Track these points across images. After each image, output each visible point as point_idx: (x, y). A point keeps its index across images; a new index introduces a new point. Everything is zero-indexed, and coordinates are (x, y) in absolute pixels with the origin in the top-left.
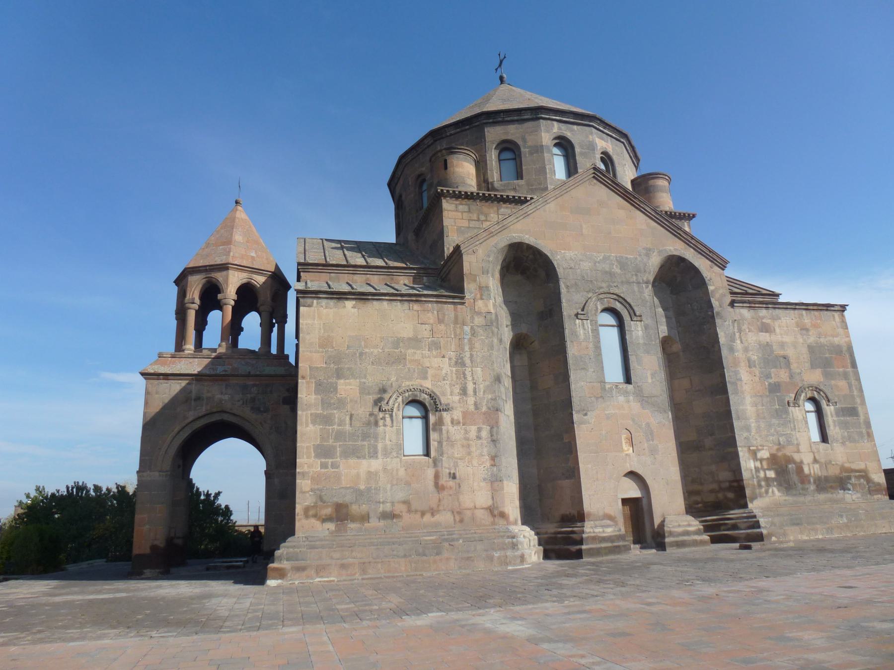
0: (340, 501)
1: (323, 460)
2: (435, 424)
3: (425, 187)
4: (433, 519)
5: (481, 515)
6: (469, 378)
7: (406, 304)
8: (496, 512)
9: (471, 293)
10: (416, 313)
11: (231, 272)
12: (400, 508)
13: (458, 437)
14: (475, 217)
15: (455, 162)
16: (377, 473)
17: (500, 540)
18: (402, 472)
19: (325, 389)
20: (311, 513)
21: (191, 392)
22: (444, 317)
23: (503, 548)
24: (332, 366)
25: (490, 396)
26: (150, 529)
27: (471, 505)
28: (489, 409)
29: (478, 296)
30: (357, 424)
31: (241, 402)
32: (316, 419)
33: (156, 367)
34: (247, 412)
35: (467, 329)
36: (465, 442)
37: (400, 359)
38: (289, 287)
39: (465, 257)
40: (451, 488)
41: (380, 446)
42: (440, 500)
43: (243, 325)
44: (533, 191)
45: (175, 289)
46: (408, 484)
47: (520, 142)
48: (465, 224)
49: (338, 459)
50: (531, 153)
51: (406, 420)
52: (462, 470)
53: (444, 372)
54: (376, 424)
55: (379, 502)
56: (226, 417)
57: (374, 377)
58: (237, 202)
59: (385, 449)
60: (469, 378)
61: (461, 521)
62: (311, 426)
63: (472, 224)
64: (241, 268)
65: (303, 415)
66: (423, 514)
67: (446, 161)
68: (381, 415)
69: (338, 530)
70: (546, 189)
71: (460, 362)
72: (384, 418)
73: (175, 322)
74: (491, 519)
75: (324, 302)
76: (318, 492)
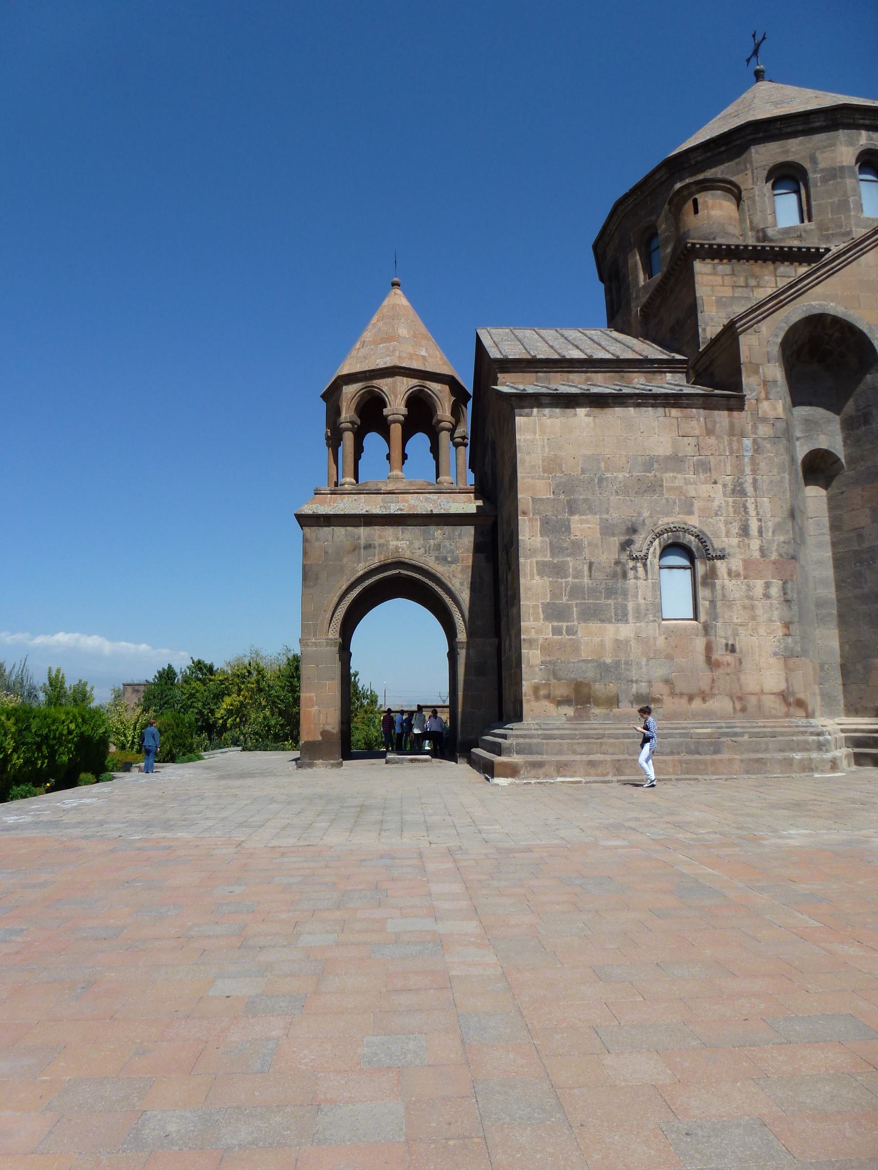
0: (579, 680)
1: (556, 624)
2: (705, 577)
4: (704, 706)
5: (771, 703)
6: (752, 513)
7: (660, 410)
8: (791, 700)
9: (752, 390)
10: (675, 421)
12: (660, 689)
13: (737, 595)
14: (741, 281)
15: (710, 202)
16: (627, 641)
17: (801, 738)
18: (661, 642)
19: (554, 528)
20: (542, 692)
21: (359, 538)
22: (714, 426)
23: (805, 747)
24: (562, 497)
25: (782, 539)
26: (320, 711)
27: (757, 689)
28: (780, 555)
29: (763, 395)
31: (422, 551)
32: (543, 569)
33: (314, 506)
35: (747, 442)
36: (747, 602)
37: (654, 487)
39: (742, 338)
40: (728, 664)
41: (630, 606)
42: (713, 681)
44: (827, 238)
45: (323, 405)
46: (670, 657)
47: (807, 165)
48: (727, 292)
49: (576, 623)
50: (824, 180)
51: (664, 572)
52: (745, 640)
53: (716, 504)
54: (625, 575)
55: (632, 681)
57: (620, 511)
59: (637, 610)
60: (752, 513)
61: (744, 710)
62: (537, 578)
63: (738, 292)
65: (527, 565)
66: (691, 698)
67: (695, 202)
68: (631, 564)
69: (578, 717)
70: (849, 233)
71: (738, 490)
72: (634, 568)
74: (784, 709)
76: (551, 667)
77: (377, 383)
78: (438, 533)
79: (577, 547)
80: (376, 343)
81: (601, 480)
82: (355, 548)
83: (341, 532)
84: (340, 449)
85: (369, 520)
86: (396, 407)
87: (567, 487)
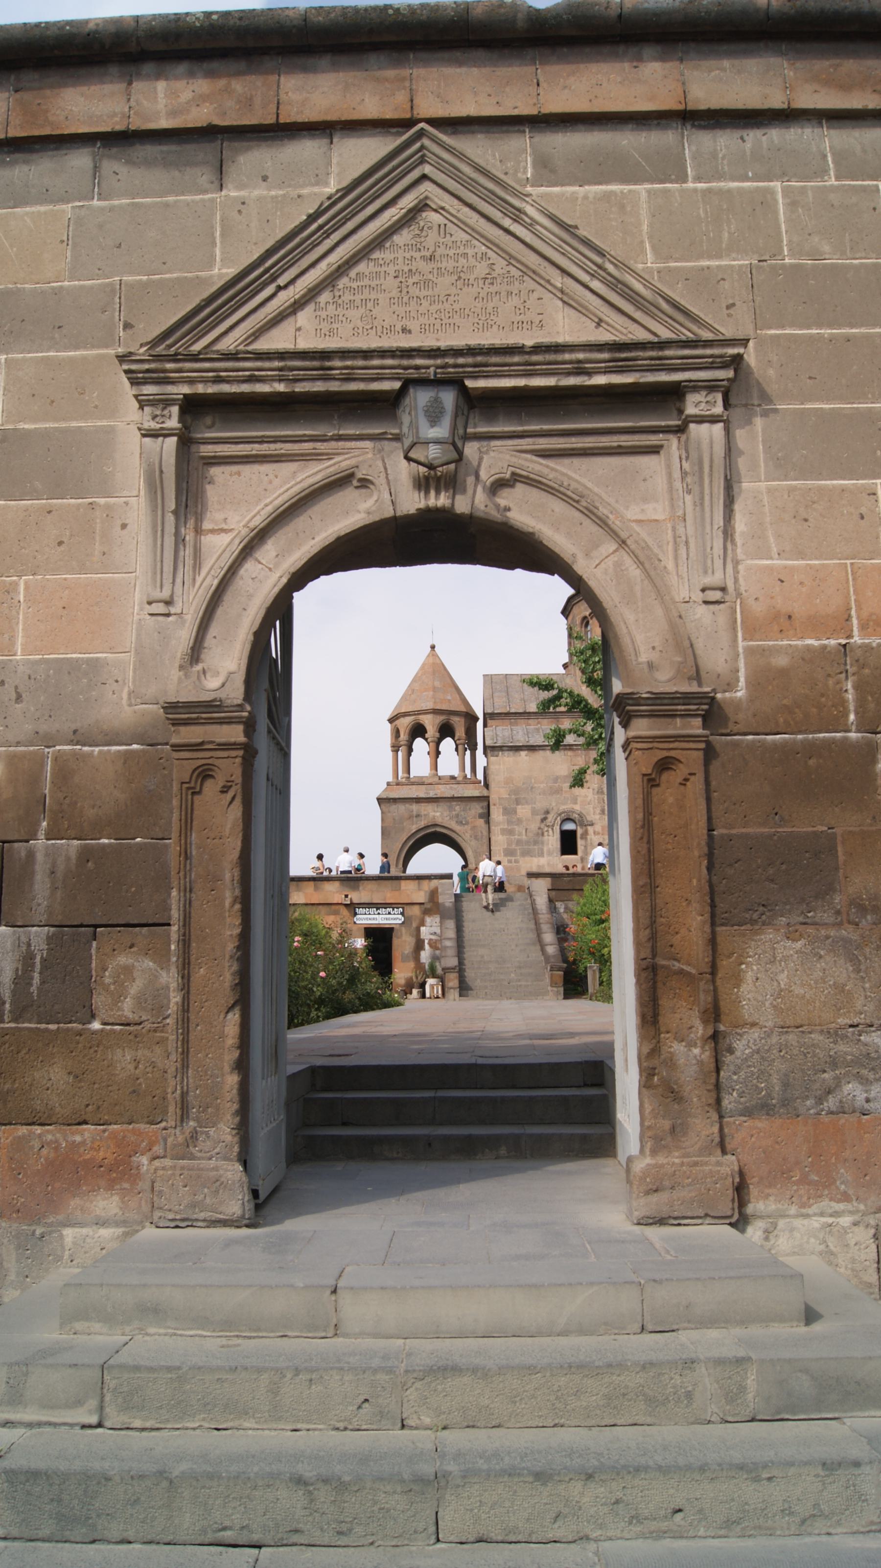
3: (589, 628)
19: (508, 812)
32: (504, 832)
34: (453, 825)
38: (477, 719)
41: (545, 849)
43: (440, 749)
53: (589, 798)
54: (543, 834)
56: (439, 829)
57: (541, 803)
68: (546, 829)
72: (548, 831)
75: (506, 753)
78: (458, 808)
79: (520, 821)
81: (532, 788)
83: (402, 808)
85: (418, 800)
86: (432, 731)
87: (516, 791)
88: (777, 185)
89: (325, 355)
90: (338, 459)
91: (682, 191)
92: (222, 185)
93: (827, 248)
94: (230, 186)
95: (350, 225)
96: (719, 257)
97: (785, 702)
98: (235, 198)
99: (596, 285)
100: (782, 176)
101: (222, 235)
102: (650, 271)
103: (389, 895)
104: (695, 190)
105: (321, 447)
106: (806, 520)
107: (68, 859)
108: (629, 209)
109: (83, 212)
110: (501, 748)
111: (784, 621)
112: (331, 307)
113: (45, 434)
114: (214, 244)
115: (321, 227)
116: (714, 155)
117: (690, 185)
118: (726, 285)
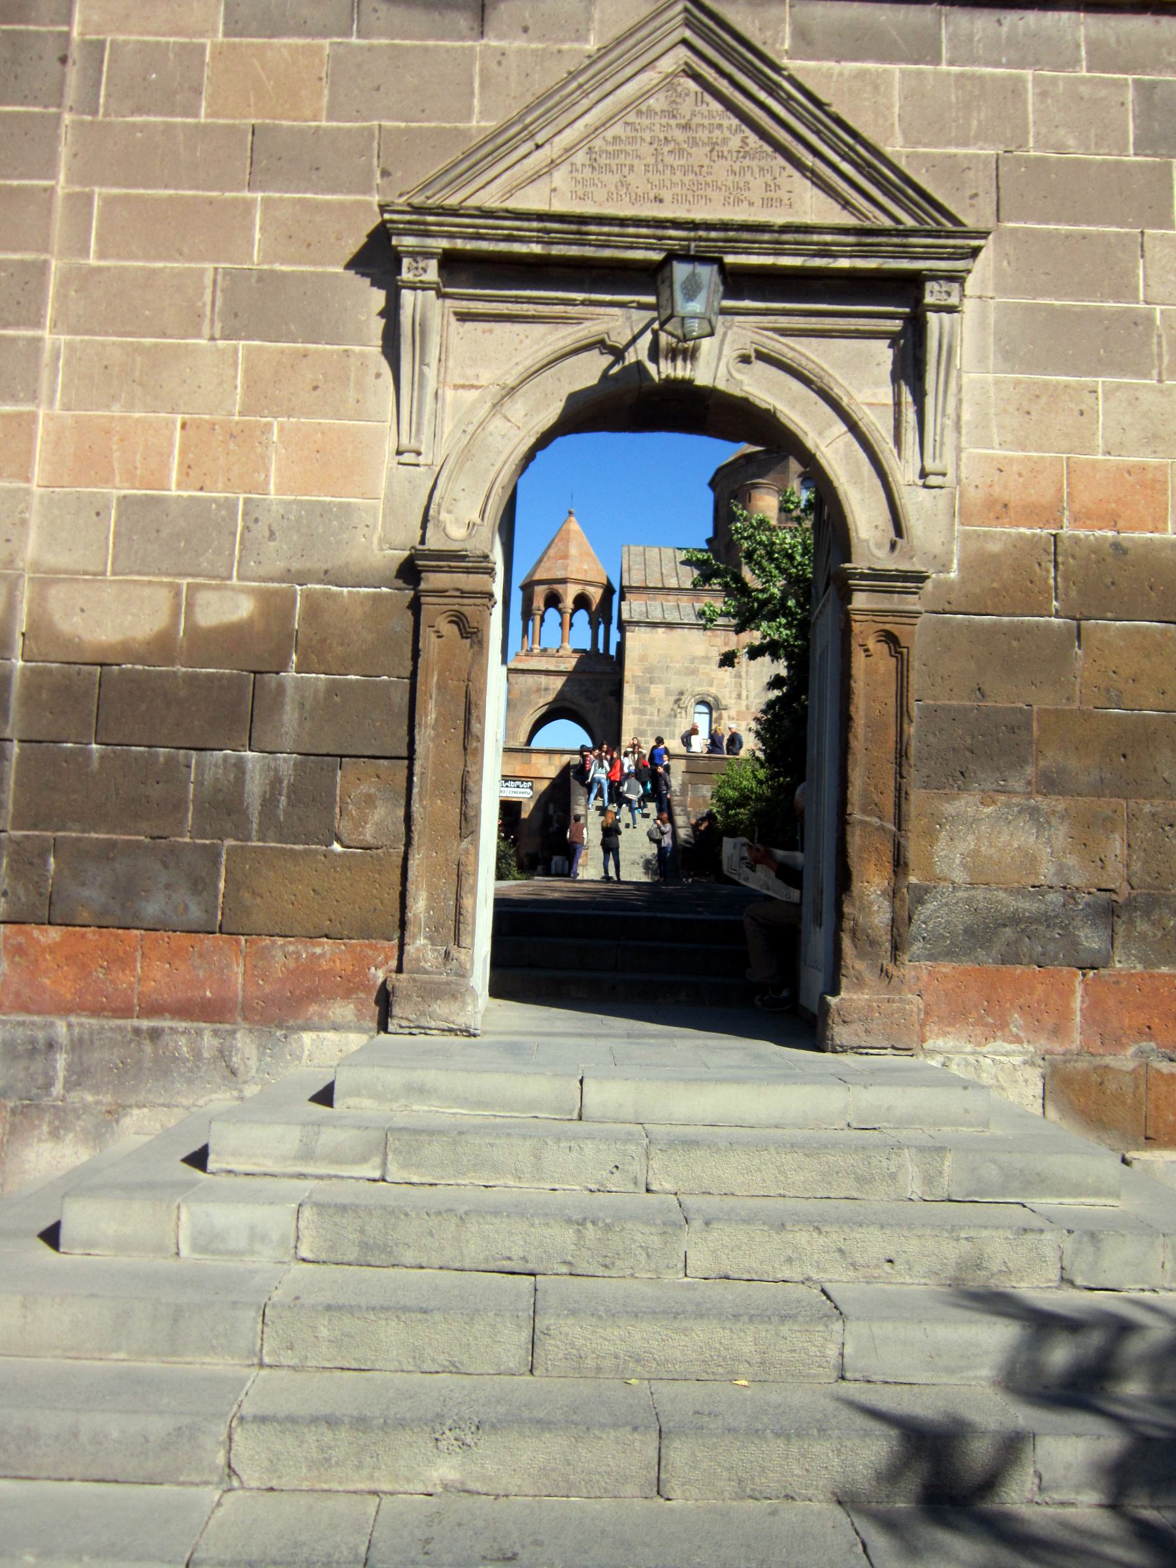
11: (569, 585)
19: (641, 690)
30: (663, 715)
32: (636, 711)
37: (694, 672)
54: (675, 716)
56: (566, 704)
57: (676, 683)
58: (570, 513)
60: (744, 686)
64: (577, 582)
65: (627, 708)
73: (521, 623)
75: (643, 629)
77: (556, 587)
79: (652, 701)
80: (557, 559)
82: (539, 690)
83: (530, 679)
84: (531, 623)
85: (547, 673)
87: (650, 670)
88: (1028, 74)
89: (583, 220)
90: (587, 324)
91: (936, 74)
92: (482, 33)
93: (1071, 142)
94: (491, 34)
95: (608, 86)
96: (966, 144)
97: (995, 585)
98: (495, 48)
99: (845, 167)
100: (1036, 63)
101: (482, 86)
102: (899, 154)
103: (518, 768)
104: (949, 74)
105: (571, 310)
106: (1028, 413)
107: (316, 692)
108: (882, 89)
109: (342, 49)
110: (637, 623)
111: (1000, 510)
112: (588, 170)
113: (302, 277)
114: (472, 93)
115: (580, 86)
116: (970, 37)
117: (944, 67)
118: (971, 174)
